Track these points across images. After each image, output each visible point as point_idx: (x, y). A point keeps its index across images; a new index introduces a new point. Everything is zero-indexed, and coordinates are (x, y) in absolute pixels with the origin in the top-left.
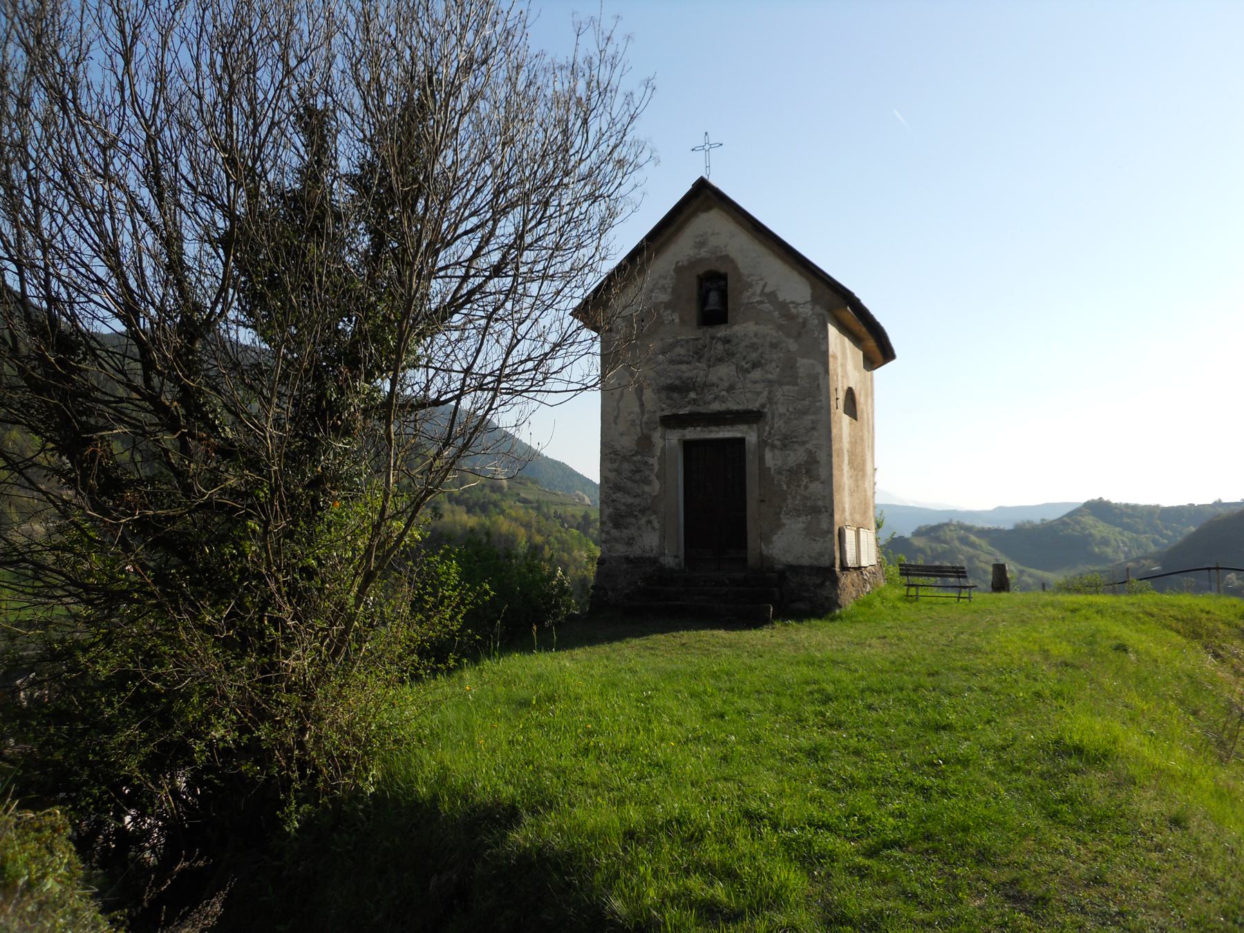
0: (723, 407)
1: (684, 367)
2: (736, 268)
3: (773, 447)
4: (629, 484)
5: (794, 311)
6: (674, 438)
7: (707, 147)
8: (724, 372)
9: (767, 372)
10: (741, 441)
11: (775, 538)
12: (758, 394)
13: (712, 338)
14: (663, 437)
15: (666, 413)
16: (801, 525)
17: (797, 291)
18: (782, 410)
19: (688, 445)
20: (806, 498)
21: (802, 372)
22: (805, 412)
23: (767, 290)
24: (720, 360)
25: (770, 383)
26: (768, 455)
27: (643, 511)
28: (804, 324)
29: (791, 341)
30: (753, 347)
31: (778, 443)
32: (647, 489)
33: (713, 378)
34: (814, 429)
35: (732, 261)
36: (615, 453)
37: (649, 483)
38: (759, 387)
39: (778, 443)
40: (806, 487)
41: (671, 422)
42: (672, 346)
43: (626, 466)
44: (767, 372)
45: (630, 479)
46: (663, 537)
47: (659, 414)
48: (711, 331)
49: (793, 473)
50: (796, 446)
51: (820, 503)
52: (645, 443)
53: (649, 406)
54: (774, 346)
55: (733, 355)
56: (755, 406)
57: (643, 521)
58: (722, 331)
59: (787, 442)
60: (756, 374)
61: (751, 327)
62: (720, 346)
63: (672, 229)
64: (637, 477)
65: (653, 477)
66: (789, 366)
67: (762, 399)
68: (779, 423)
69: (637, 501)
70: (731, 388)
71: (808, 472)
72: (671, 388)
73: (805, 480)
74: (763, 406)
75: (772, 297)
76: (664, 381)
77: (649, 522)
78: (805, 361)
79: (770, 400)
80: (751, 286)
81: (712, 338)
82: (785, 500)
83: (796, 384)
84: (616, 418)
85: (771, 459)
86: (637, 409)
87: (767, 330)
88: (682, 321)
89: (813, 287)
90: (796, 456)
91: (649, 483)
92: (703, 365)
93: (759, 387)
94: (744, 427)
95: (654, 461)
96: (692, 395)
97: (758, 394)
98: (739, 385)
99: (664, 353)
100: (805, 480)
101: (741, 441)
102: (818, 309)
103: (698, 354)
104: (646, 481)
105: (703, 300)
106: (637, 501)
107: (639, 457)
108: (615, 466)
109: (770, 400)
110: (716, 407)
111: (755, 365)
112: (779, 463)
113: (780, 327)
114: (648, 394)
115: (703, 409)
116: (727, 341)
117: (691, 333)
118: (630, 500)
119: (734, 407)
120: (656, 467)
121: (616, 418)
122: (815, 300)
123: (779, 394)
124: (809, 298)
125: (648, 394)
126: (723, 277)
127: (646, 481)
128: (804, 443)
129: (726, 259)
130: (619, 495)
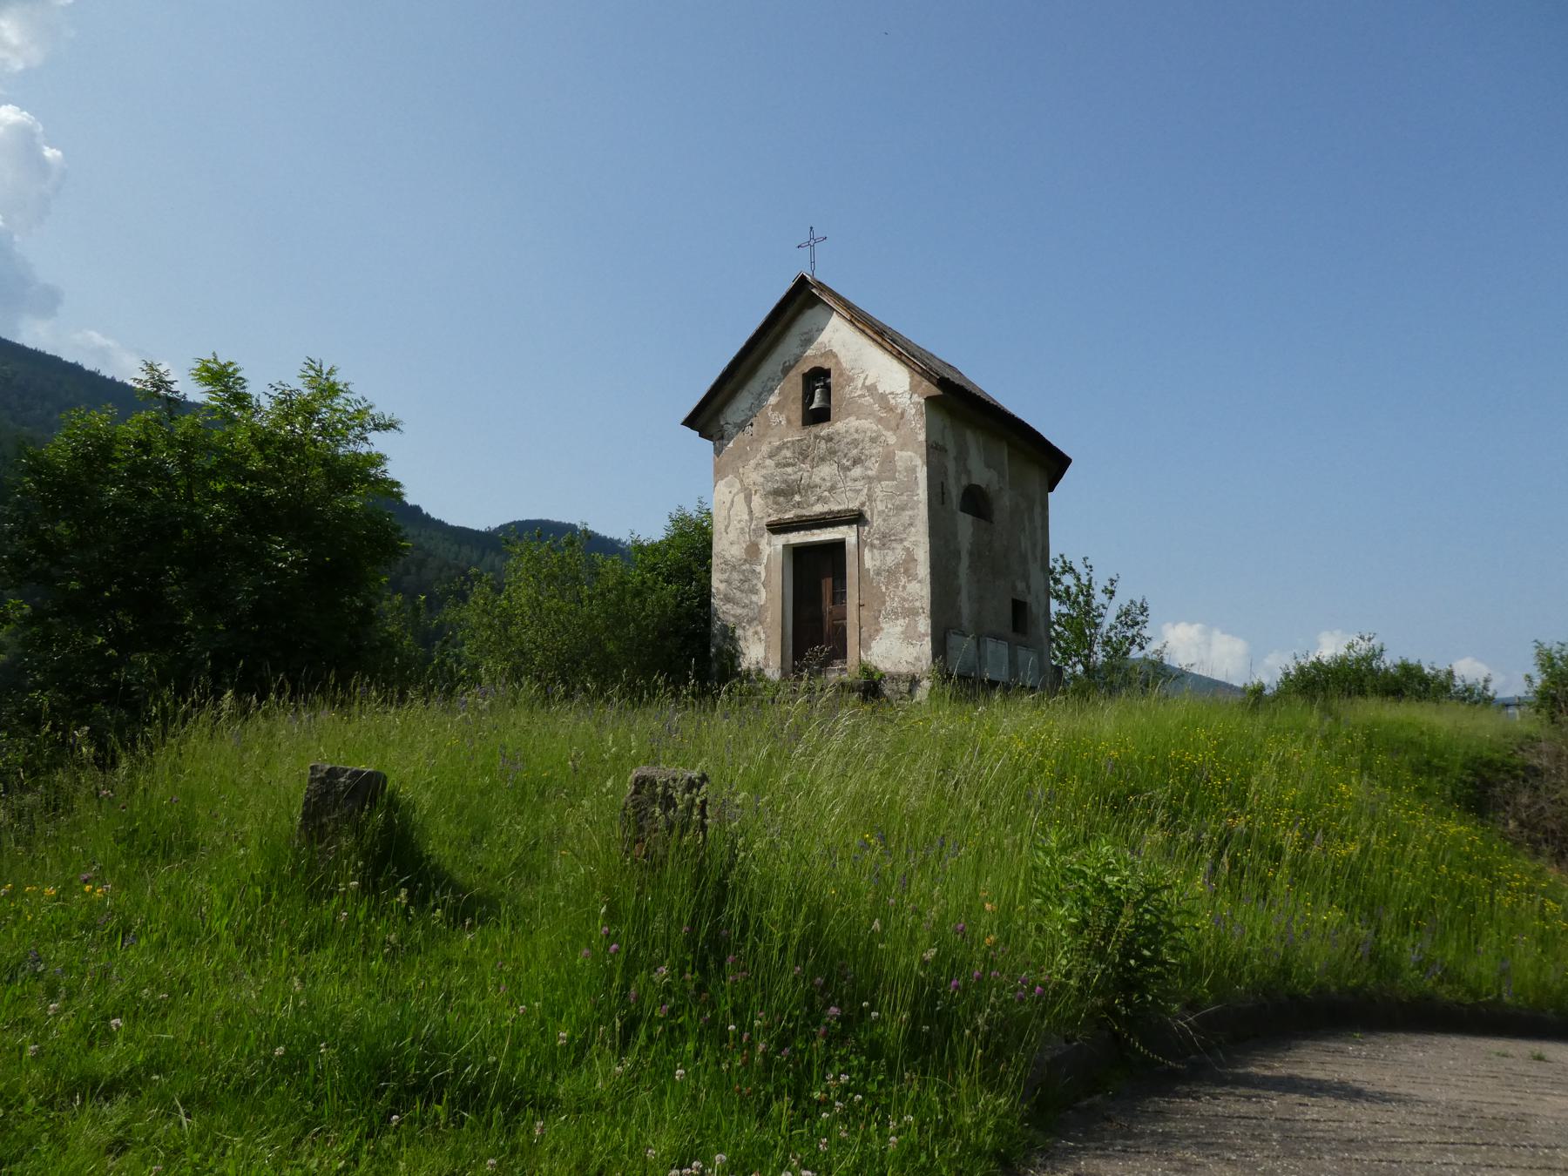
0: (825, 508)
1: (789, 470)
2: (838, 363)
3: (872, 546)
4: (738, 594)
5: (892, 402)
6: (780, 540)
7: (812, 242)
8: (827, 471)
9: (867, 468)
10: (840, 545)
11: (874, 644)
12: (858, 491)
13: (816, 437)
14: (769, 543)
15: (774, 518)
16: (899, 629)
17: (894, 379)
18: (880, 506)
19: (799, 555)
20: (905, 600)
21: (900, 465)
22: (902, 508)
23: (868, 383)
24: (823, 459)
25: (870, 479)
26: (867, 554)
27: (750, 622)
28: (902, 415)
29: (889, 434)
30: (855, 443)
31: (876, 542)
32: (754, 598)
33: (817, 480)
34: (911, 525)
35: (835, 356)
36: (725, 562)
37: (756, 592)
38: (859, 485)
39: (876, 542)
40: (904, 587)
41: (777, 528)
42: (779, 449)
43: (735, 576)
44: (867, 468)
45: (738, 588)
46: (767, 648)
47: (766, 520)
48: (815, 429)
49: (892, 574)
50: (894, 545)
51: (918, 604)
52: (753, 551)
53: (757, 514)
54: (873, 440)
55: (835, 453)
56: (854, 505)
57: (750, 633)
58: (824, 430)
59: (886, 540)
60: (857, 471)
61: (853, 422)
62: (823, 445)
63: (778, 328)
64: (746, 586)
65: (760, 586)
66: (888, 459)
67: (862, 497)
68: (877, 522)
69: (745, 611)
70: (832, 489)
71: (906, 571)
72: (777, 493)
73: (903, 580)
74: (863, 504)
75: (872, 389)
76: (770, 486)
77: (756, 633)
78: (904, 454)
79: (870, 497)
80: (851, 379)
81: (816, 437)
82: (884, 603)
83: (894, 479)
84: (727, 527)
85: (870, 560)
86: (746, 517)
87: (867, 424)
88: (789, 421)
89: (912, 377)
90: (894, 556)
91: (756, 592)
92: (806, 466)
93: (859, 485)
94: (844, 529)
95: (761, 569)
96: (797, 498)
97: (858, 491)
98: (840, 485)
99: (770, 457)
100: (903, 580)
101: (840, 545)
102: (916, 398)
103: (803, 455)
104: (754, 591)
105: (808, 396)
106: (745, 611)
107: (746, 567)
108: (725, 576)
109: (870, 497)
110: (819, 509)
111: (855, 463)
112: (878, 563)
113: (880, 420)
114: (757, 501)
115: (806, 512)
116: (829, 439)
117: (795, 435)
118: (739, 611)
119: (836, 508)
120: (763, 575)
121: (727, 527)
122: (913, 389)
123: (878, 491)
124: (907, 387)
125: (757, 501)
126: (826, 373)
127: (754, 591)
128: (902, 540)
129: (831, 354)
130: (729, 606)
